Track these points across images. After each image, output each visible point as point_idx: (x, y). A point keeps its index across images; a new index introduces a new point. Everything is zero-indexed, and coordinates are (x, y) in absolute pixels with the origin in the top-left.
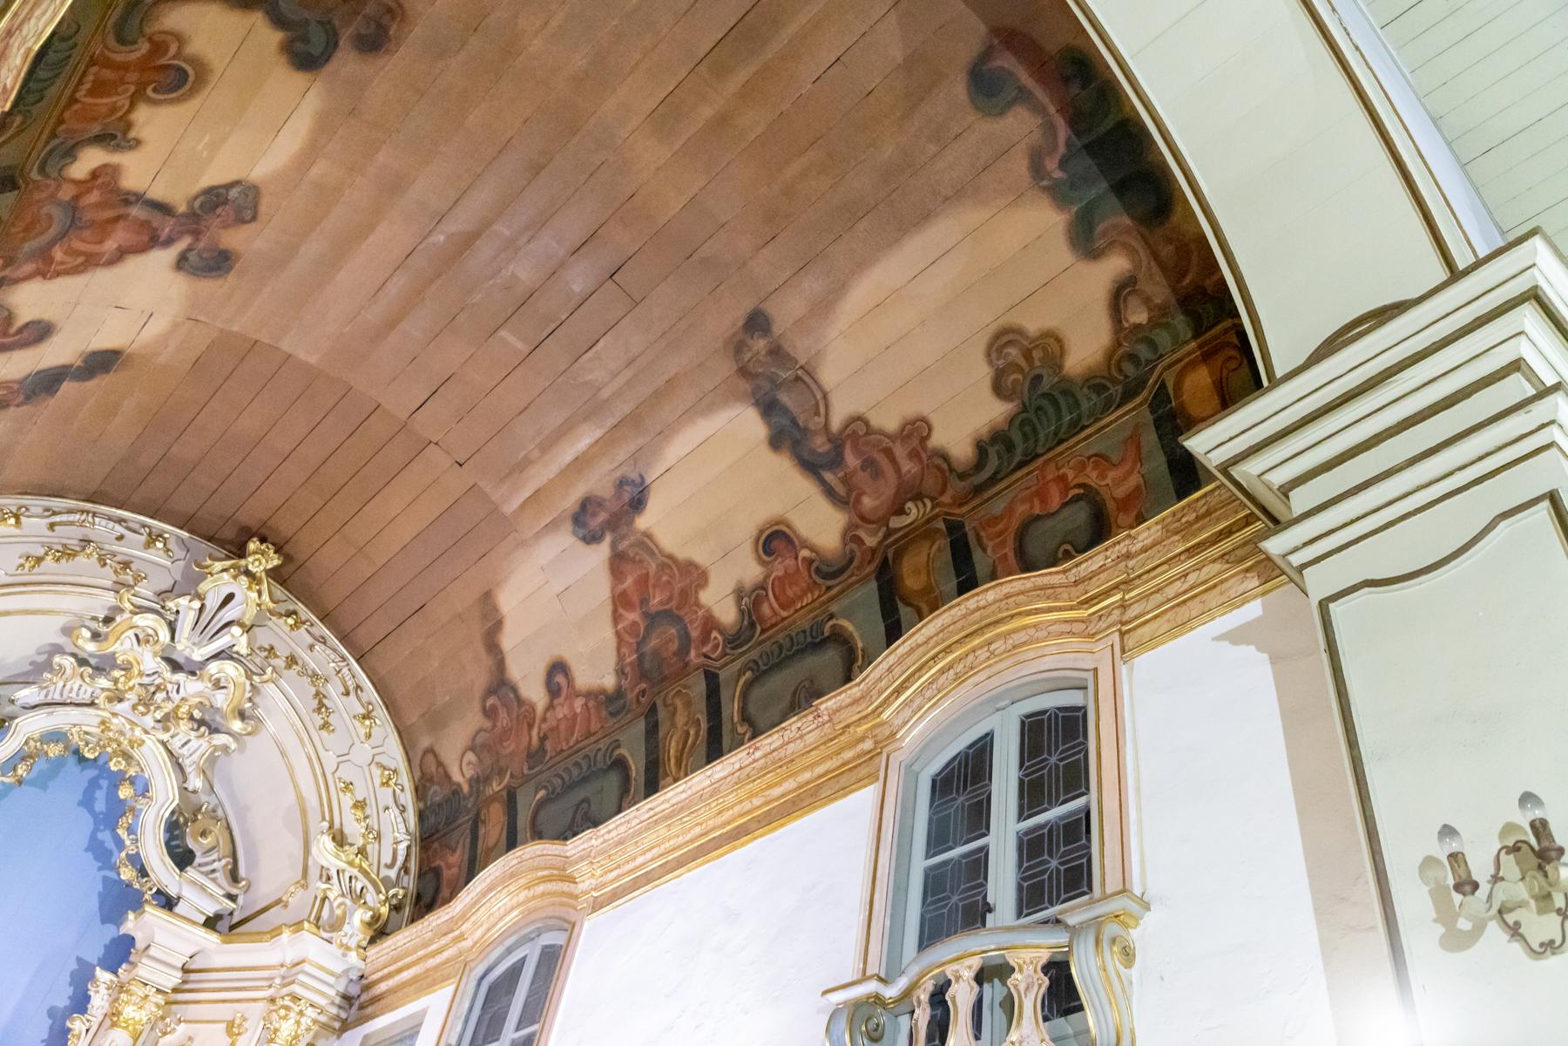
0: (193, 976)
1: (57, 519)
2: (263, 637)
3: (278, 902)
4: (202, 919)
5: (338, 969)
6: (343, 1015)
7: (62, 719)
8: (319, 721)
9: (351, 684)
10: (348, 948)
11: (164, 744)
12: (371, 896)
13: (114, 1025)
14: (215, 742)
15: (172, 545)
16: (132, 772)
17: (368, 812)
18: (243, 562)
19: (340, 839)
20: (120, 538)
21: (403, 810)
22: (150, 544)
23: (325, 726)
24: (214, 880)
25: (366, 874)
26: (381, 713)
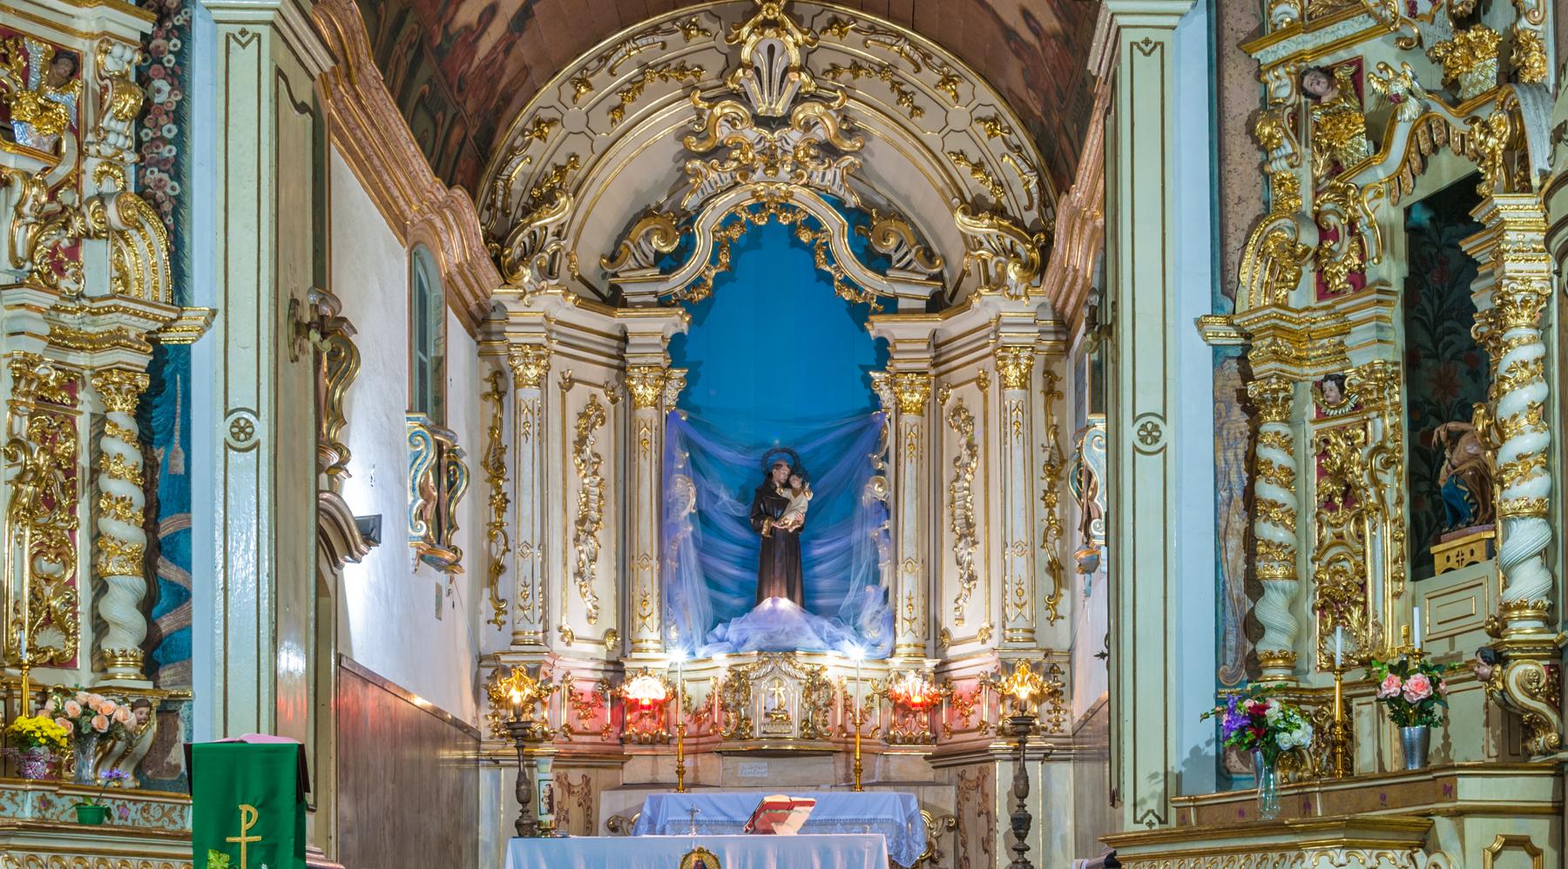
0: (944, 349)
1: (611, 62)
2: (821, 61)
3: (964, 272)
4: (922, 305)
5: (1033, 308)
6: (1063, 338)
7: (724, 202)
8: (905, 107)
9: (916, 57)
10: (1018, 297)
11: (806, 185)
12: (1019, 248)
13: (902, 411)
14: (844, 164)
15: (705, 24)
16: (800, 217)
17: (988, 168)
18: (760, 17)
19: (975, 208)
20: (664, 45)
21: (1019, 149)
22: (687, 37)
23: (916, 110)
24: (913, 271)
25: (1009, 231)
26: (960, 66)
